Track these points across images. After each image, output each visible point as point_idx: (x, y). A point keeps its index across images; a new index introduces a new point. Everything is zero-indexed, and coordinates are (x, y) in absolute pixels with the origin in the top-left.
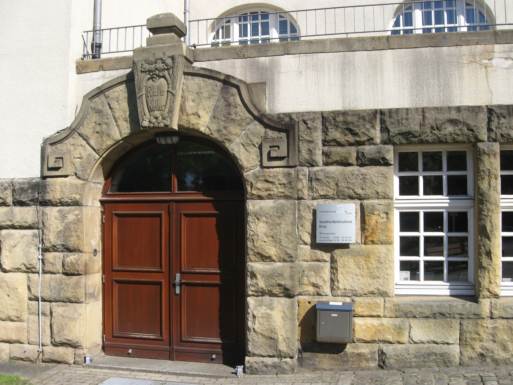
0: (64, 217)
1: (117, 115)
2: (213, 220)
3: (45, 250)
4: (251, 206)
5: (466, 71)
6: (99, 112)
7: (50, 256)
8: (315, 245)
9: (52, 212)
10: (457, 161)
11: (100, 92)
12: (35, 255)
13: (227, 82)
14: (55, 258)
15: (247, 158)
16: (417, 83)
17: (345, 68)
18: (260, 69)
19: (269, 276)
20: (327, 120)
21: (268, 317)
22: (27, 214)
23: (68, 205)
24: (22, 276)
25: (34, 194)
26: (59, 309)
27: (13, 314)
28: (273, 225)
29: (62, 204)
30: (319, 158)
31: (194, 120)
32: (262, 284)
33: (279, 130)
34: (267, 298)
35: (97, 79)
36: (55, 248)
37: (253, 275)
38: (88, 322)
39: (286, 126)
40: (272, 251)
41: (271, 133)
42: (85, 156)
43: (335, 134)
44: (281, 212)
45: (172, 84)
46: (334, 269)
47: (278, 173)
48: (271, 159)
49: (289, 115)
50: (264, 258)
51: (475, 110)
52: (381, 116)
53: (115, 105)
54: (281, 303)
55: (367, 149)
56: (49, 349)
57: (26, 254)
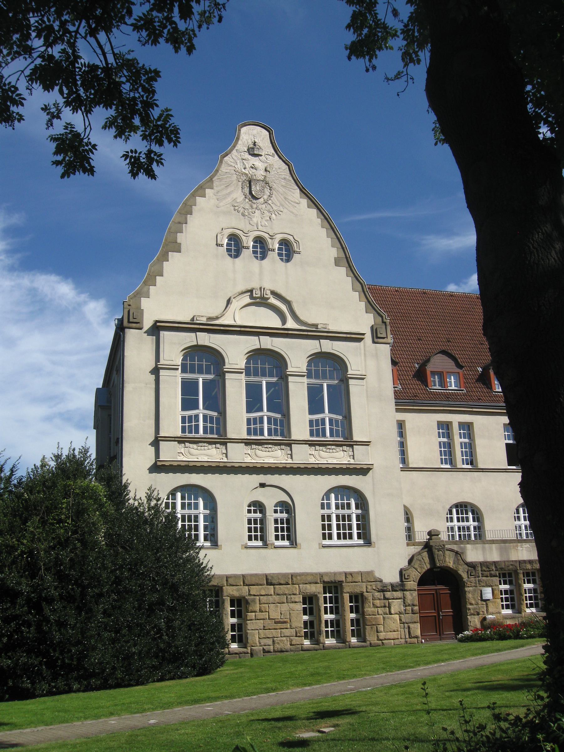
0: (412, 595)
1: (426, 561)
2: (448, 595)
3: (406, 606)
4: (467, 589)
5: (512, 551)
6: (420, 560)
7: (408, 608)
8: (482, 600)
9: (407, 593)
10: (510, 575)
11: (419, 553)
12: (403, 608)
13: (457, 553)
14: (409, 608)
15: (464, 576)
16: (501, 555)
17: (484, 549)
18: (461, 548)
19: (474, 609)
20: (482, 564)
21: (474, 621)
22: (399, 594)
23: (412, 590)
24: (398, 616)
25: (401, 587)
26: (411, 626)
27: (396, 629)
28: (473, 595)
29: (410, 590)
30: (480, 575)
31: (449, 564)
32: (472, 612)
33: (472, 567)
34: (473, 616)
35: (413, 550)
36: (409, 605)
37: (469, 609)
38: (417, 629)
39: (472, 566)
40: (473, 602)
41: (470, 568)
42: (415, 575)
43: (484, 568)
44: (475, 590)
45: (444, 553)
46: (487, 607)
47: (472, 579)
48: (471, 575)
49: (472, 562)
50: (471, 604)
51: (516, 561)
52: (495, 563)
53: (424, 558)
54: (476, 617)
55: (492, 572)
56: (409, 640)
57: (400, 608)
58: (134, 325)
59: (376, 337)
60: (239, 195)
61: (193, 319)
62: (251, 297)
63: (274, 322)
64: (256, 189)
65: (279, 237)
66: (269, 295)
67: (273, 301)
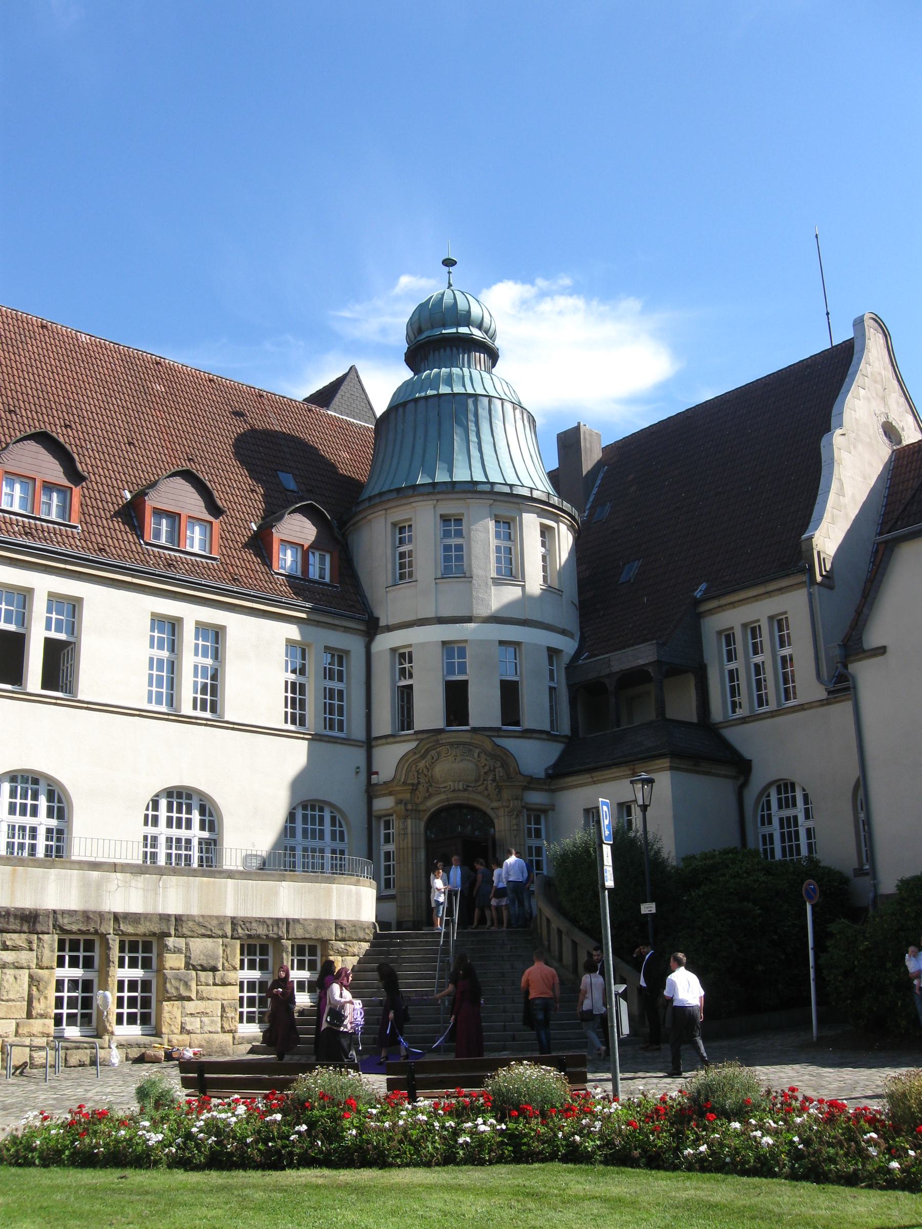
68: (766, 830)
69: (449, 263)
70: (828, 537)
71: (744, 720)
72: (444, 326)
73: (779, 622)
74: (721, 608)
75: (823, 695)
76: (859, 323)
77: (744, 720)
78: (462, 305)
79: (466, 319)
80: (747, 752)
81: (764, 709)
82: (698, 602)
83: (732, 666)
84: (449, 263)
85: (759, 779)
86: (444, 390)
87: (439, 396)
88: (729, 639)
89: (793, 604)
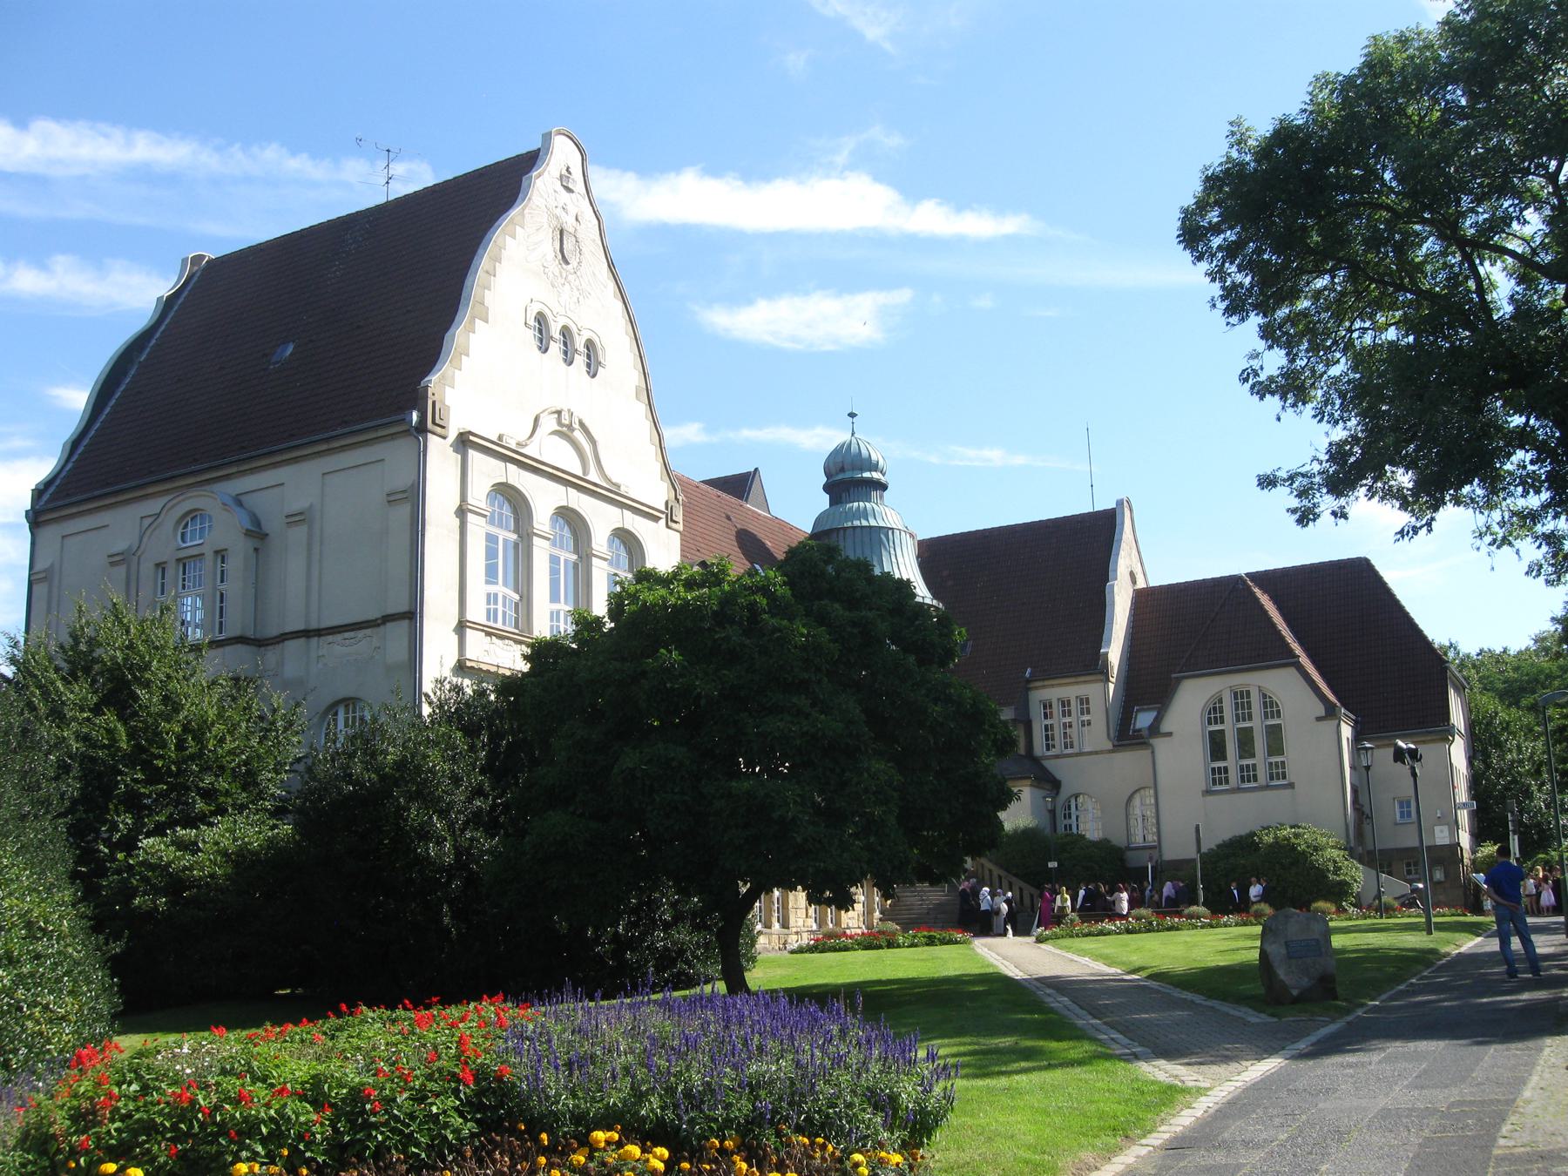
58: (438, 430)
59: (670, 519)
60: (549, 248)
61: (500, 437)
62: (559, 423)
63: (571, 463)
64: (569, 245)
65: (586, 335)
66: (576, 426)
67: (578, 435)
68: (1067, 822)
69: (852, 415)
70: (1115, 652)
71: (1057, 757)
72: (862, 470)
73: (1084, 701)
74: (1044, 687)
75: (1109, 746)
76: (1120, 503)
77: (1057, 757)
78: (874, 457)
79: (874, 467)
80: (1058, 777)
81: (1069, 751)
82: (1028, 681)
83: (1048, 722)
84: (852, 415)
85: (1065, 792)
86: (873, 523)
87: (870, 527)
88: (1047, 705)
89: (1090, 689)
